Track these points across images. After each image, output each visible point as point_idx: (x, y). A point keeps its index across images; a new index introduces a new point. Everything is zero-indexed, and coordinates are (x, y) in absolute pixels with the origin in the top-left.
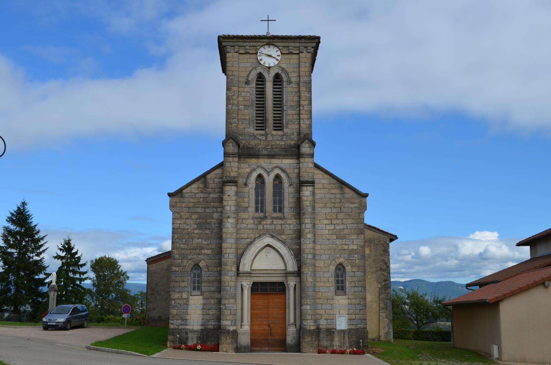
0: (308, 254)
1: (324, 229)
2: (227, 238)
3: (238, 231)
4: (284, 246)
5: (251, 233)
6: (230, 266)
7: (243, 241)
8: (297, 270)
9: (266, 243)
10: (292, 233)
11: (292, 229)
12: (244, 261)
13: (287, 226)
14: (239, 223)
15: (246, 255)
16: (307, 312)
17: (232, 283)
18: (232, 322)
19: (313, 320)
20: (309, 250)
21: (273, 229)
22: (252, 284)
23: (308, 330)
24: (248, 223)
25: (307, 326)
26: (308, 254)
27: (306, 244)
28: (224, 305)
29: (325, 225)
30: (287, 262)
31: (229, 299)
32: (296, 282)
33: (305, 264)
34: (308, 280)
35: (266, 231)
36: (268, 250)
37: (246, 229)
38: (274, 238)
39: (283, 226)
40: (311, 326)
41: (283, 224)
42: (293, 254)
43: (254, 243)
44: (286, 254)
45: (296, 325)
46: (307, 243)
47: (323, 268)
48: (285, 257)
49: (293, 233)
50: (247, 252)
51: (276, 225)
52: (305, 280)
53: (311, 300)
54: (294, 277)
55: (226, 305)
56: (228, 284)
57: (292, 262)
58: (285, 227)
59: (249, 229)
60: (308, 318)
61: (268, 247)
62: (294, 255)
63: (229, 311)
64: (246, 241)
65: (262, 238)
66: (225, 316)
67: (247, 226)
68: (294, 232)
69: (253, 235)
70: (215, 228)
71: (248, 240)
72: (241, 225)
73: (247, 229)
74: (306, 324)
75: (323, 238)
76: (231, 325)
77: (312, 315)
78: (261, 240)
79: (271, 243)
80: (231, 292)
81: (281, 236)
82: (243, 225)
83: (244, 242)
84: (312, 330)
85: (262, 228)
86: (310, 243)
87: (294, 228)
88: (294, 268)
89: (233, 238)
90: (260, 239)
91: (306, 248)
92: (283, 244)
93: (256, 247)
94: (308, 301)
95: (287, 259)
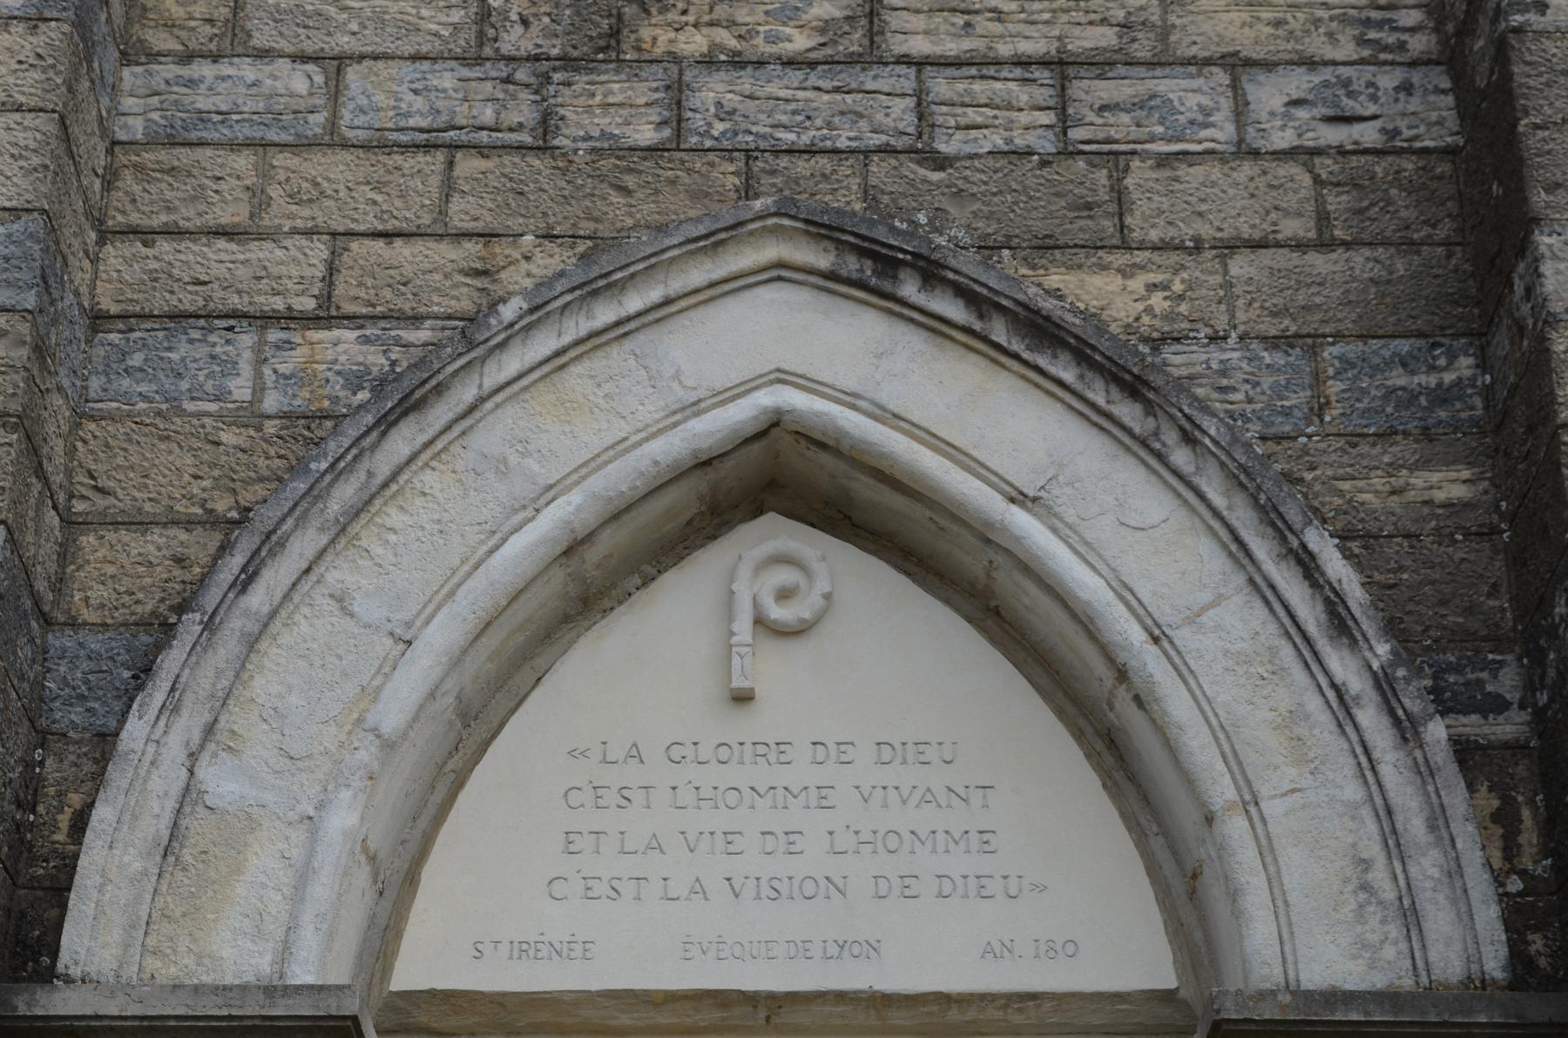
3: (128, 180)
4: (1148, 449)
7: (230, 367)
8: (1494, 962)
10: (1291, 228)
11: (1283, 139)
14: (162, 41)
15: (252, 643)
24: (344, 43)
30: (1221, 790)
35: (727, 176)
36: (784, 576)
37: (304, 145)
38: (910, 289)
39: (1105, 90)
41: (1101, 64)
42: (1355, 592)
43: (466, 393)
44: (1193, 618)
48: (1182, 671)
49: (1323, 218)
50: (277, 576)
51: (941, 86)
57: (1352, 791)
59: (379, 145)
61: (771, 520)
62: (1392, 628)
65: (634, 302)
68: (1336, 202)
69: (446, 253)
73: (333, 140)
78: (622, 329)
79: (850, 399)
81: (1054, 280)
82: (247, 70)
83: (240, 389)
85: (646, 134)
87: (1333, 135)
88: (1410, 917)
90: (605, 313)
92: (1101, 420)
93: (502, 469)
95: (1222, 733)
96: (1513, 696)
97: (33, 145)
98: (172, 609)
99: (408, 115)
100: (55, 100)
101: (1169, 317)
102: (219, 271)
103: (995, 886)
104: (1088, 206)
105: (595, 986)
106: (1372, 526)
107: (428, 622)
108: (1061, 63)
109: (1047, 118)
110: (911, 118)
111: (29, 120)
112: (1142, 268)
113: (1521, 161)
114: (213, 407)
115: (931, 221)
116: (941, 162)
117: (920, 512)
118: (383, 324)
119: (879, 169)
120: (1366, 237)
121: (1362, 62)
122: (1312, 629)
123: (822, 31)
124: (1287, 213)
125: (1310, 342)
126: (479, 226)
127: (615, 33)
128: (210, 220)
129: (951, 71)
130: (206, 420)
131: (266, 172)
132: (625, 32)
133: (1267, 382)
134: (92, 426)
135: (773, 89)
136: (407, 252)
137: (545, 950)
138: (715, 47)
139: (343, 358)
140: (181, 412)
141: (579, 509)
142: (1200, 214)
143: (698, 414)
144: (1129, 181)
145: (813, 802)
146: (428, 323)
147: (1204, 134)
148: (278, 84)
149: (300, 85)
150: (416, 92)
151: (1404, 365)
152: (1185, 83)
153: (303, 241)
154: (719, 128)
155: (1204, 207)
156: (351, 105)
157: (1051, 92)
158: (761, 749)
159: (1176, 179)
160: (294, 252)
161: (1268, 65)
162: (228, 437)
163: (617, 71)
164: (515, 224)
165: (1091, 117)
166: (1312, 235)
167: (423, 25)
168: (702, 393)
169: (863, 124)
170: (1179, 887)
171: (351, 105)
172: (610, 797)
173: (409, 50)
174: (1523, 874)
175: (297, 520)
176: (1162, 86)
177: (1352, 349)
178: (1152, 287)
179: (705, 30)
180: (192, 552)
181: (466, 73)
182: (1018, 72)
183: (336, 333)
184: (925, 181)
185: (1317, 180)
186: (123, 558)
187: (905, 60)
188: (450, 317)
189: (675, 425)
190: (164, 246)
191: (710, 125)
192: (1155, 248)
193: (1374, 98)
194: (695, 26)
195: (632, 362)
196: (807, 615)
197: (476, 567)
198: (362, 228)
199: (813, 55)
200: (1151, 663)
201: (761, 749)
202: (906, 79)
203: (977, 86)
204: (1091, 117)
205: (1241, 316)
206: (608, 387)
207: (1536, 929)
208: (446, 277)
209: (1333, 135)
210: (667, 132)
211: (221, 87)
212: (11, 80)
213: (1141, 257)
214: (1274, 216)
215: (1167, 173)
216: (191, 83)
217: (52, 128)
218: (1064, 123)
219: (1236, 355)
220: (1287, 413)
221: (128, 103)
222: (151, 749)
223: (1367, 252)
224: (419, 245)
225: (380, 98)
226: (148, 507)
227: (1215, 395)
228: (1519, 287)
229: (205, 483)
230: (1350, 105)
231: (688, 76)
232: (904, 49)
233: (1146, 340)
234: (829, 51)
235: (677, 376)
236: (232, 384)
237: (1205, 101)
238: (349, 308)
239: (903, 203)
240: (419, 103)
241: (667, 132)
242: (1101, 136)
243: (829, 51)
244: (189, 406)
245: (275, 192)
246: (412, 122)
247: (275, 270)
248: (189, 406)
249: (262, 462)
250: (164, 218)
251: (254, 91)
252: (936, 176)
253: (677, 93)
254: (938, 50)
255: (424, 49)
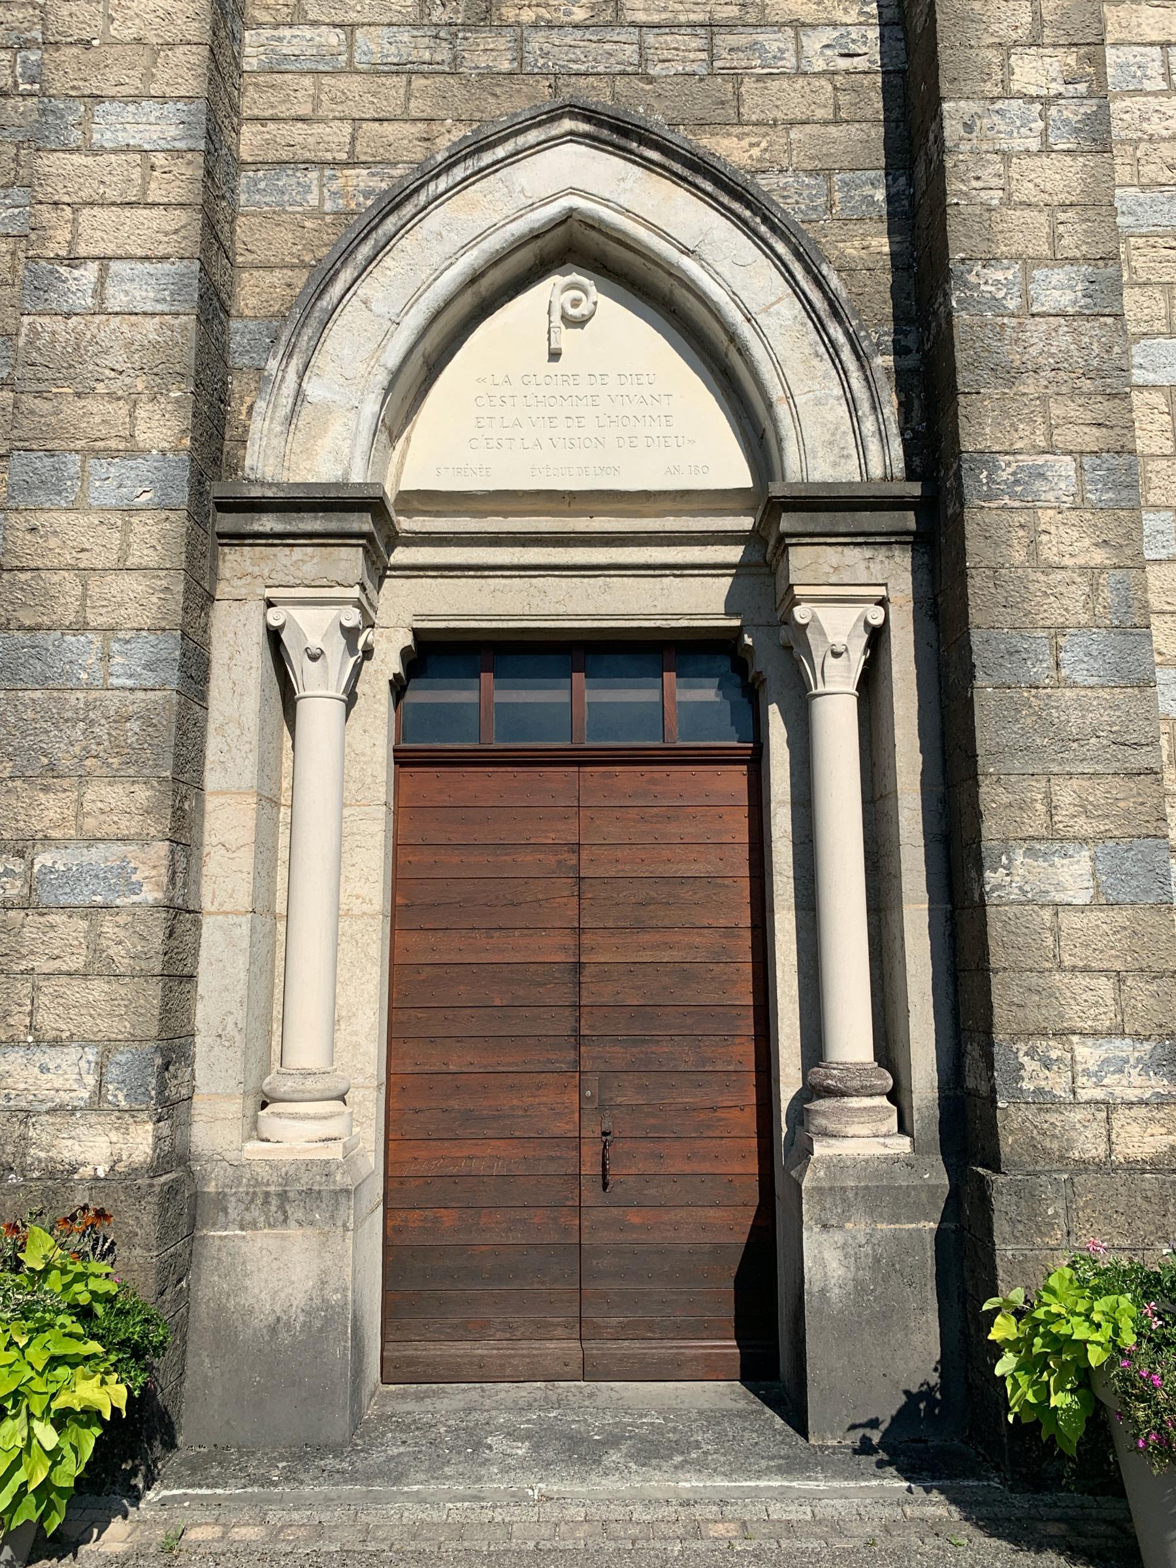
0: (1038, 261)
1: (1148, 86)
2: (98, 98)
5: (388, 110)
6: (113, 397)
7: (307, 189)
8: (899, 468)
9: (547, 201)
10: (820, 113)
11: (819, 65)
12: (301, 377)
13: (772, 41)
16: (1056, 931)
17: (134, 585)
18: (113, 1072)
19: (1137, 1037)
20: (1043, 218)
21: (619, 68)
22: (405, 653)
23: (1083, 1166)
24: (353, 17)
25: (1077, 1115)
26: (1038, 261)
27: (1006, 156)
28: (21, 854)
29: (1156, 52)
30: (776, 392)
31: (84, 778)
32: (883, 602)
33: (1010, 375)
34: (1049, 553)
36: (577, 294)
39: (733, 40)
40: (1120, 1117)
41: (730, 26)
44: (766, 310)
45: (893, 1096)
46: (1017, 144)
47: (1164, 463)
49: (837, 108)
51: (650, 38)
52: (1019, 555)
53: (1098, 793)
54: (868, 552)
55: (44, 859)
56: (84, 596)
58: (753, 47)
59: (375, 72)
60: (1074, 1017)
63: (73, 929)
64: (335, 186)
66: (23, 989)
67: (351, 46)
70: (21, 87)
71: (359, 178)
72: (286, 32)
74: (1057, 1083)
75: (1149, 171)
76: (97, 1102)
77: (1120, 978)
80: (113, 700)
82: (307, 32)
84: (1134, 1167)
85: (506, 66)
86: (1046, 150)
87: (844, 64)
89: (163, 98)
91: (1007, 202)
94: (1066, 795)
96: (914, 347)
97: (197, 62)
98: (287, 309)
99: (387, 56)
100: (207, 38)
101: (760, 160)
102: (300, 139)
103: (670, 441)
104: (723, 103)
105: (491, 488)
106: (853, 265)
107: (407, 313)
108: (710, 26)
109: (704, 55)
110: (636, 56)
111: (194, 48)
112: (747, 135)
113: (937, 67)
114: (300, 209)
115: (645, 111)
116: (651, 80)
117: (639, 261)
118: (380, 166)
119: (620, 82)
120: (857, 118)
121: (860, 24)
122: (822, 314)
123: (592, 9)
124: (819, 106)
125: (825, 173)
126: (424, 115)
127: (488, 11)
128: (292, 113)
129: (656, 31)
130: (298, 216)
131: (318, 87)
132: (494, 9)
133: (805, 193)
134: (244, 219)
135: (569, 40)
136: (390, 129)
137: (469, 472)
138: (538, 17)
139: (362, 184)
140: (285, 212)
141: (477, 258)
142: (777, 107)
143: (531, 211)
144: (743, 89)
145: (590, 402)
146: (400, 166)
147: (780, 63)
148: (323, 40)
149: (334, 40)
150: (390, 43)
151: (872, 184)
152: (772, 36)
153: (338, 123)
154: (541, 62)
155: (779, 103)
156: (359, 51)
157: (705, 41)
158: (565, 378)
159: (766, 88)
160: (335, 129)
161: (813, 26)
162: (307, 224)
163: (490, 31)
164: (442, 114)
165: (725, 55)
166: (831, 117)
167: (393, 7)
168: (535, 200)
169: (612, 60)
170: (755, 442)
171: (359, 51)
172: (497, 401)
173: (387, 21)
174: (912, 430)
175: (342, 263)
176: (761, 38)
177: (847, 176)
178: (752, 145)
179: (534, 9)
180: (294, 281)
181: (415, 33)
182: (689, 30)
183: (358, 171)
184: (642, 90)
185: (835, 88)
186: (262, 283)
187: (633, 24)
188: (412, 163)
189: (521, 216)
190: (271, 126)
191: (536, 60)
192: (754, 125)
193: (865, 43)
194: (529, 6)
195: (500, 184)
196: (586, 313)
197: (429, 287)
198: (368, 116)
199: (588, 23)
200: (745, 331)
201: (565, 378)
202: (633, 35)
203: (669, 38)
204: (725, 55)
205: (795, 159)
206: (489, 197)
207: (917, 455)
208: (410, 141)
209: (844, 64)
210: (516, 64)
211: (294, 41)
212: (184, 27)
213: (747, 129)
214: (813, 107)
215: (761, 85)
216: (280, 39)
217: (206, 53)
218: (712, 58)
219: (791, 179)
220: (815, 208)
221: (248, 50)
222: (280, 374)
223: (857, 125)
224: (396, 125)
225: (373, 47)
226: (272, 259)
227: (781, 200)
228: (931, 137)
229: (299, 247)
230: (853, 48)
231: (525, 34)
232: (633, 19)
233: (748, 172)
234: (595, 20)
235: (522, 191)
236: (309, 197)
237: (782, 45)
238: (363, 158)
239: (631, 101)
240: (393, 49)
241: (516, 64)
242: (728, 65)
243: (595, 20)
244: (289, 209)
245: (324, 97)
246: (389, 60)
247: (326, 139)
248: (289, 209)
249: (325, 236)
250: (270, 112)
251: (311, 43)
252: (648, 87)
253: (520, 42)
254: (650, 19)
255: (394, 20)
